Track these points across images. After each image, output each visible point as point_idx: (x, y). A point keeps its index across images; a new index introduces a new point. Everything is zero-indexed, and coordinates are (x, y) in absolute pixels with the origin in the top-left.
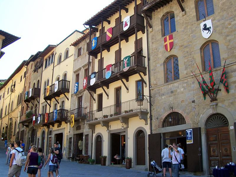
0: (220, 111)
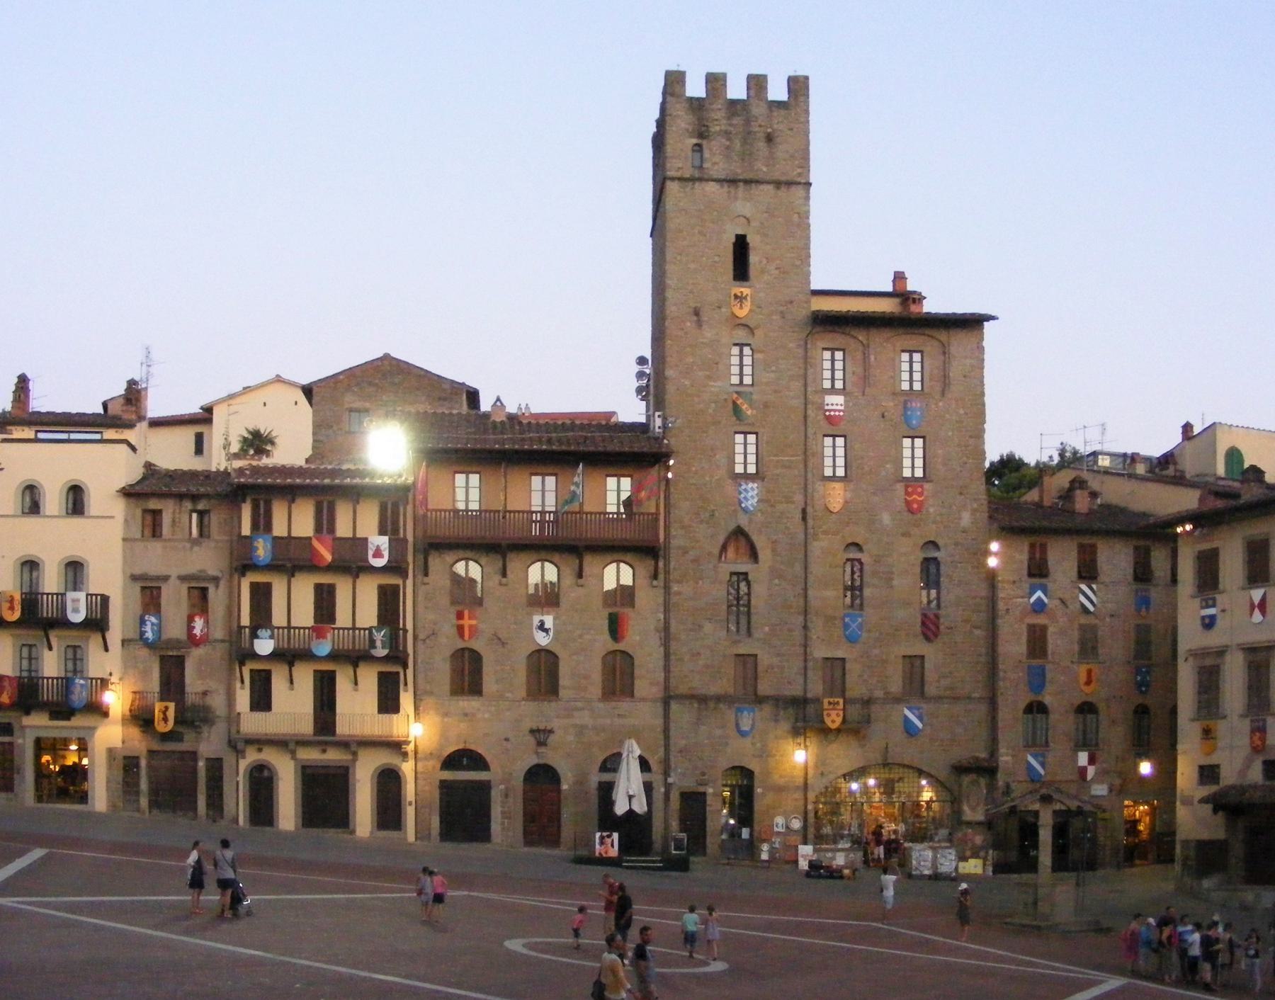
0: (550, 763)
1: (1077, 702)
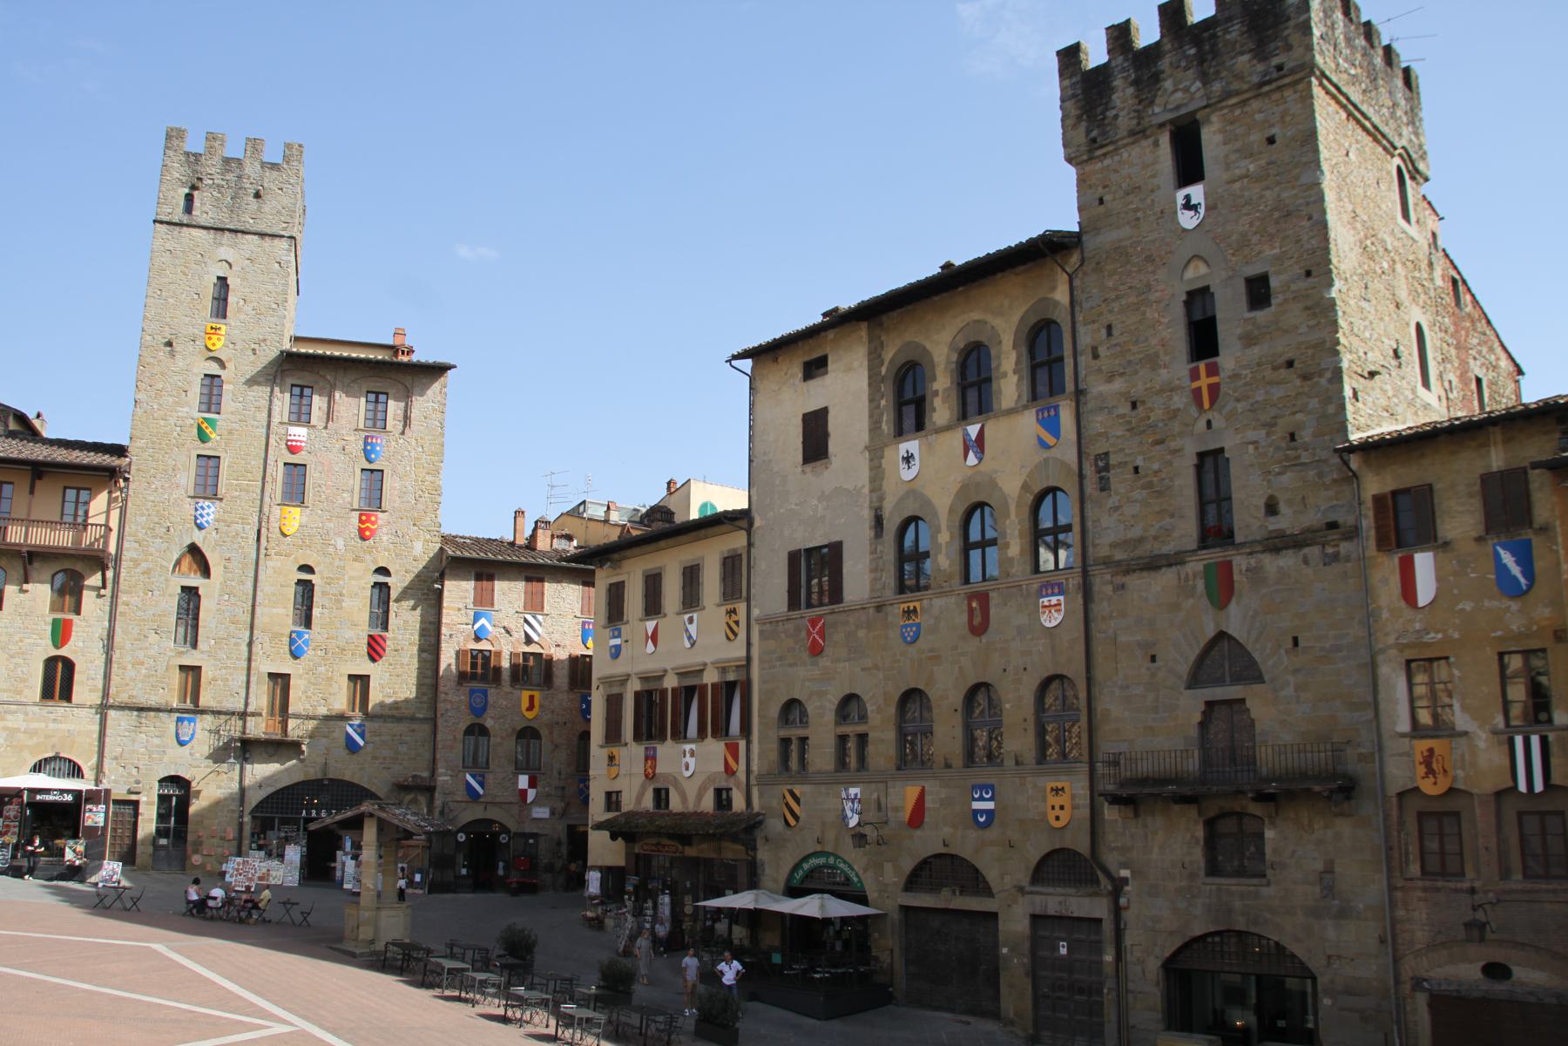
1: (519, 728)
